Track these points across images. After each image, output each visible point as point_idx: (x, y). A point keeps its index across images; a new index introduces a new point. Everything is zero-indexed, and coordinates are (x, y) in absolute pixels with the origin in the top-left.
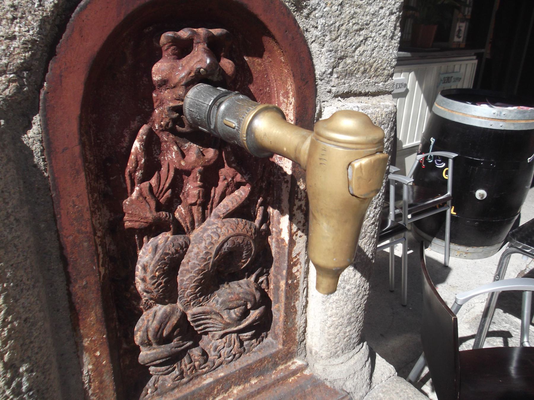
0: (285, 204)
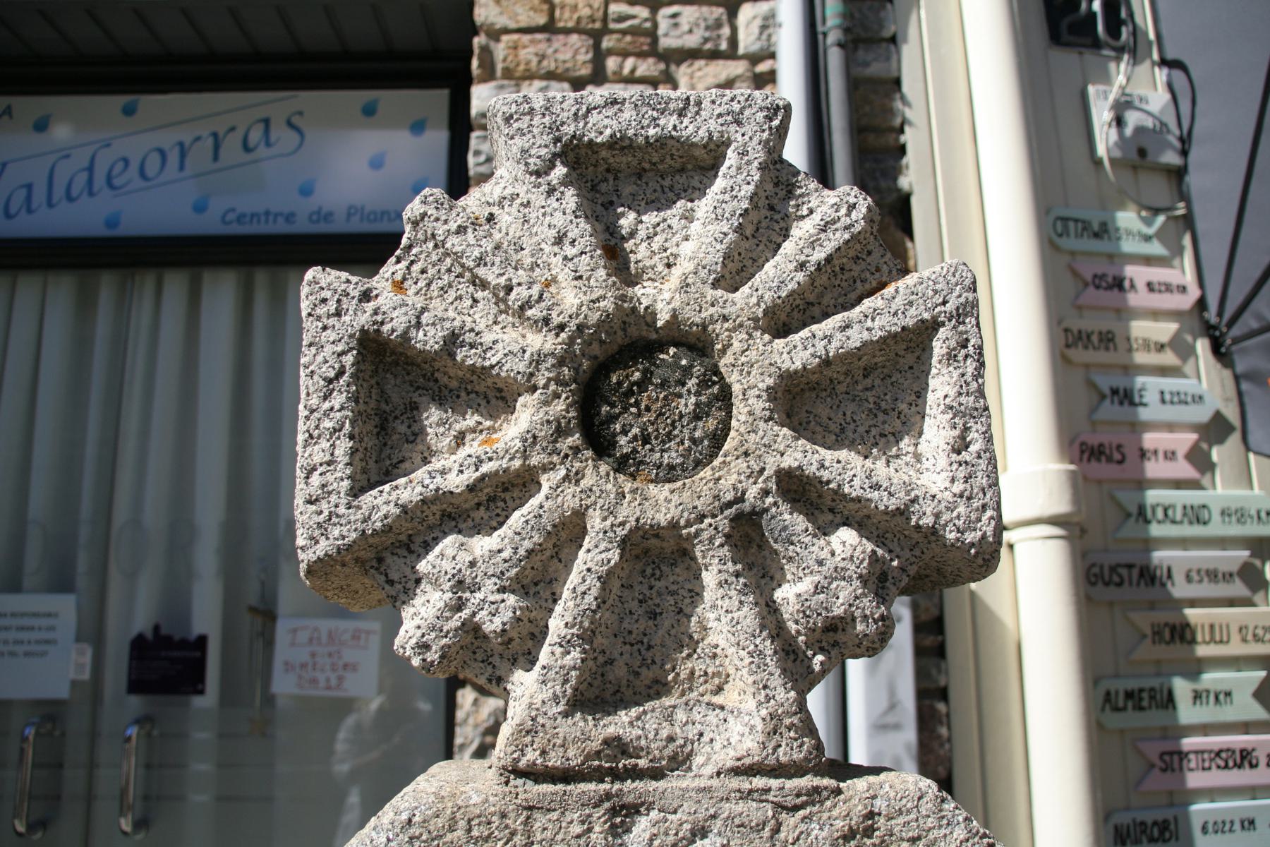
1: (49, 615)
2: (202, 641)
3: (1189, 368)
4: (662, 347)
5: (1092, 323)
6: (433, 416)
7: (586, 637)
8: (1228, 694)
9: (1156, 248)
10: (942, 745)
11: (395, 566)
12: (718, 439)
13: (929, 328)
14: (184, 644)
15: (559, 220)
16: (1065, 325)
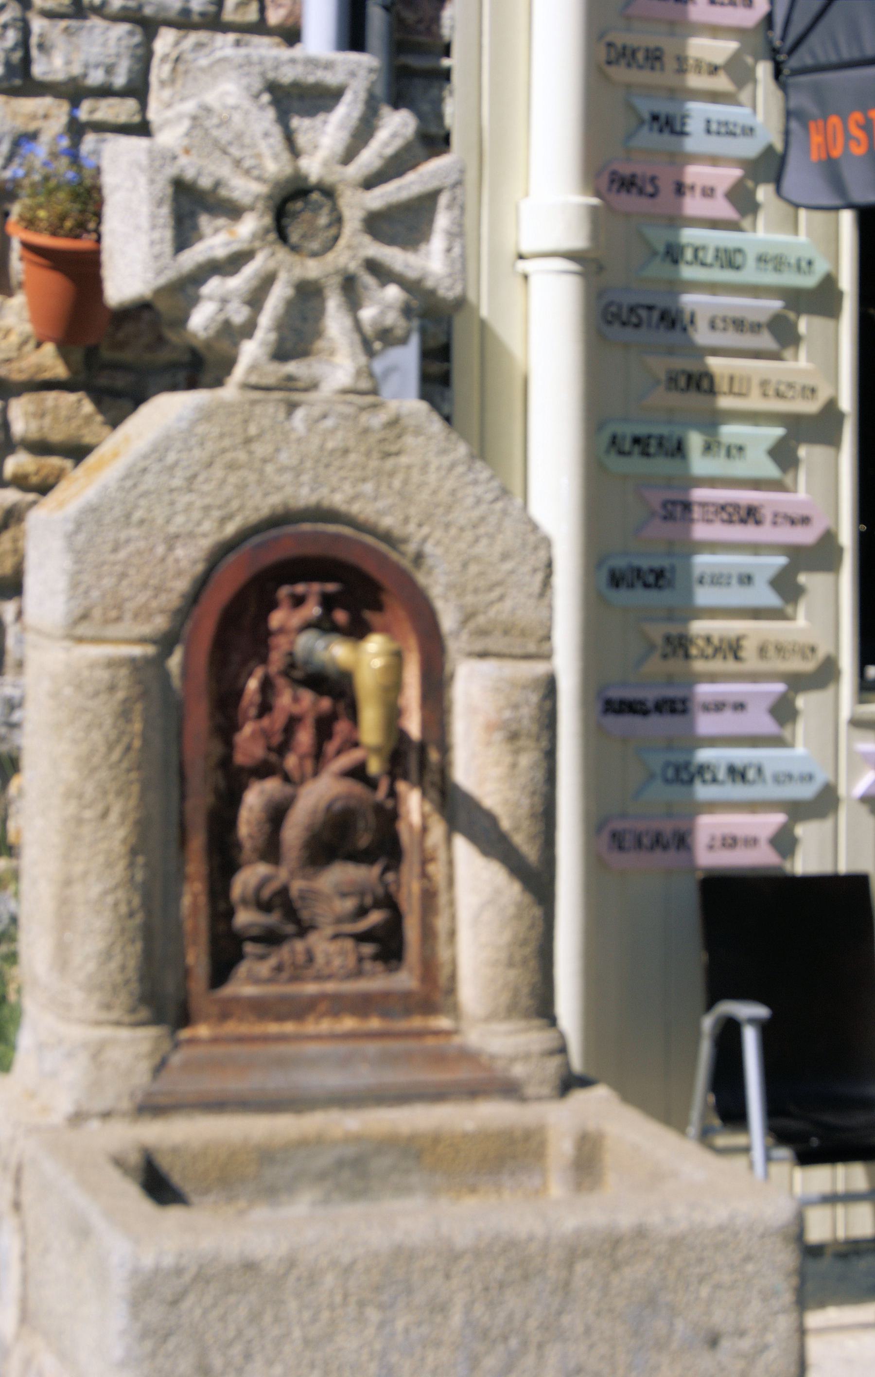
8: (741, 449)
16: (610, 38)
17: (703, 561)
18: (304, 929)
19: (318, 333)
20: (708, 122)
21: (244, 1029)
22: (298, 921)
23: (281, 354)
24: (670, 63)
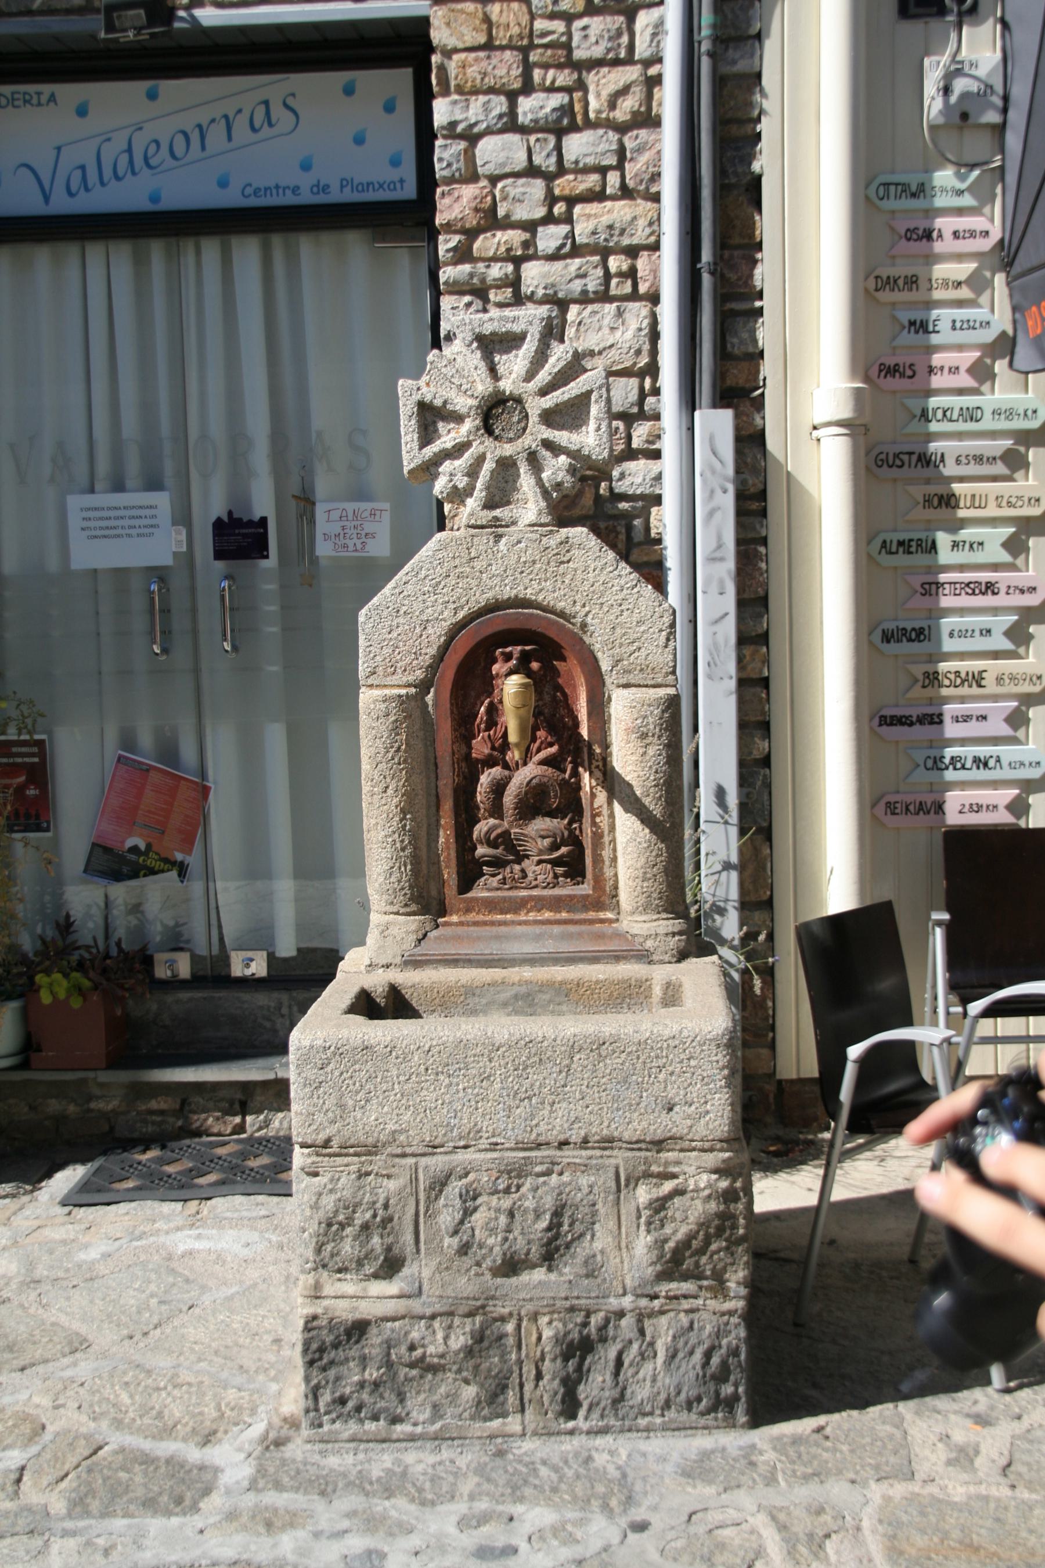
0: (586, 763)
1: (151, 507)
2: (264, 521)
3: (984, 299)
4: (508, 401)
5: (900, 270)
6: (440, 425)
7: (488, 488)
8: (981, 544)
9: (968, 200)
10: (761, 574)
11: (432, 470)
12: (524, 429)
13: (589, 393)
14: (251, 523)
15: (475, 362)
17: (948, 623)
18: (520, 858)
19: (516, 489)
20: (954, 321)
21: (481, 918)
22: (517, 853)
23: (490, 504)
24: (923, 284)
